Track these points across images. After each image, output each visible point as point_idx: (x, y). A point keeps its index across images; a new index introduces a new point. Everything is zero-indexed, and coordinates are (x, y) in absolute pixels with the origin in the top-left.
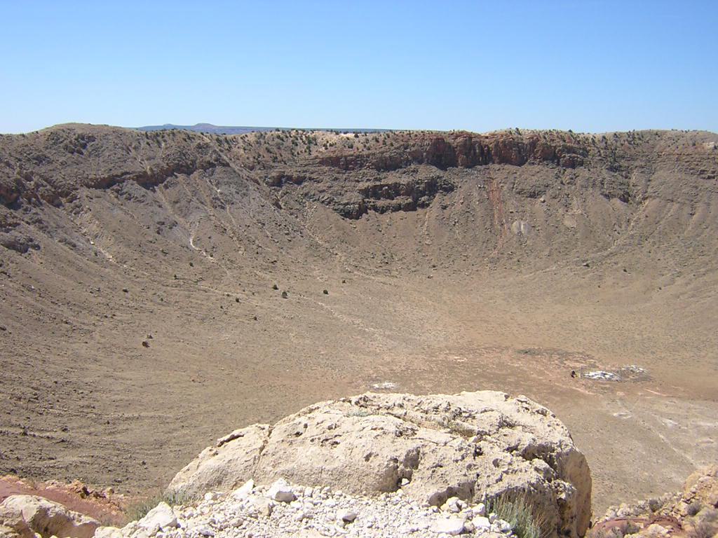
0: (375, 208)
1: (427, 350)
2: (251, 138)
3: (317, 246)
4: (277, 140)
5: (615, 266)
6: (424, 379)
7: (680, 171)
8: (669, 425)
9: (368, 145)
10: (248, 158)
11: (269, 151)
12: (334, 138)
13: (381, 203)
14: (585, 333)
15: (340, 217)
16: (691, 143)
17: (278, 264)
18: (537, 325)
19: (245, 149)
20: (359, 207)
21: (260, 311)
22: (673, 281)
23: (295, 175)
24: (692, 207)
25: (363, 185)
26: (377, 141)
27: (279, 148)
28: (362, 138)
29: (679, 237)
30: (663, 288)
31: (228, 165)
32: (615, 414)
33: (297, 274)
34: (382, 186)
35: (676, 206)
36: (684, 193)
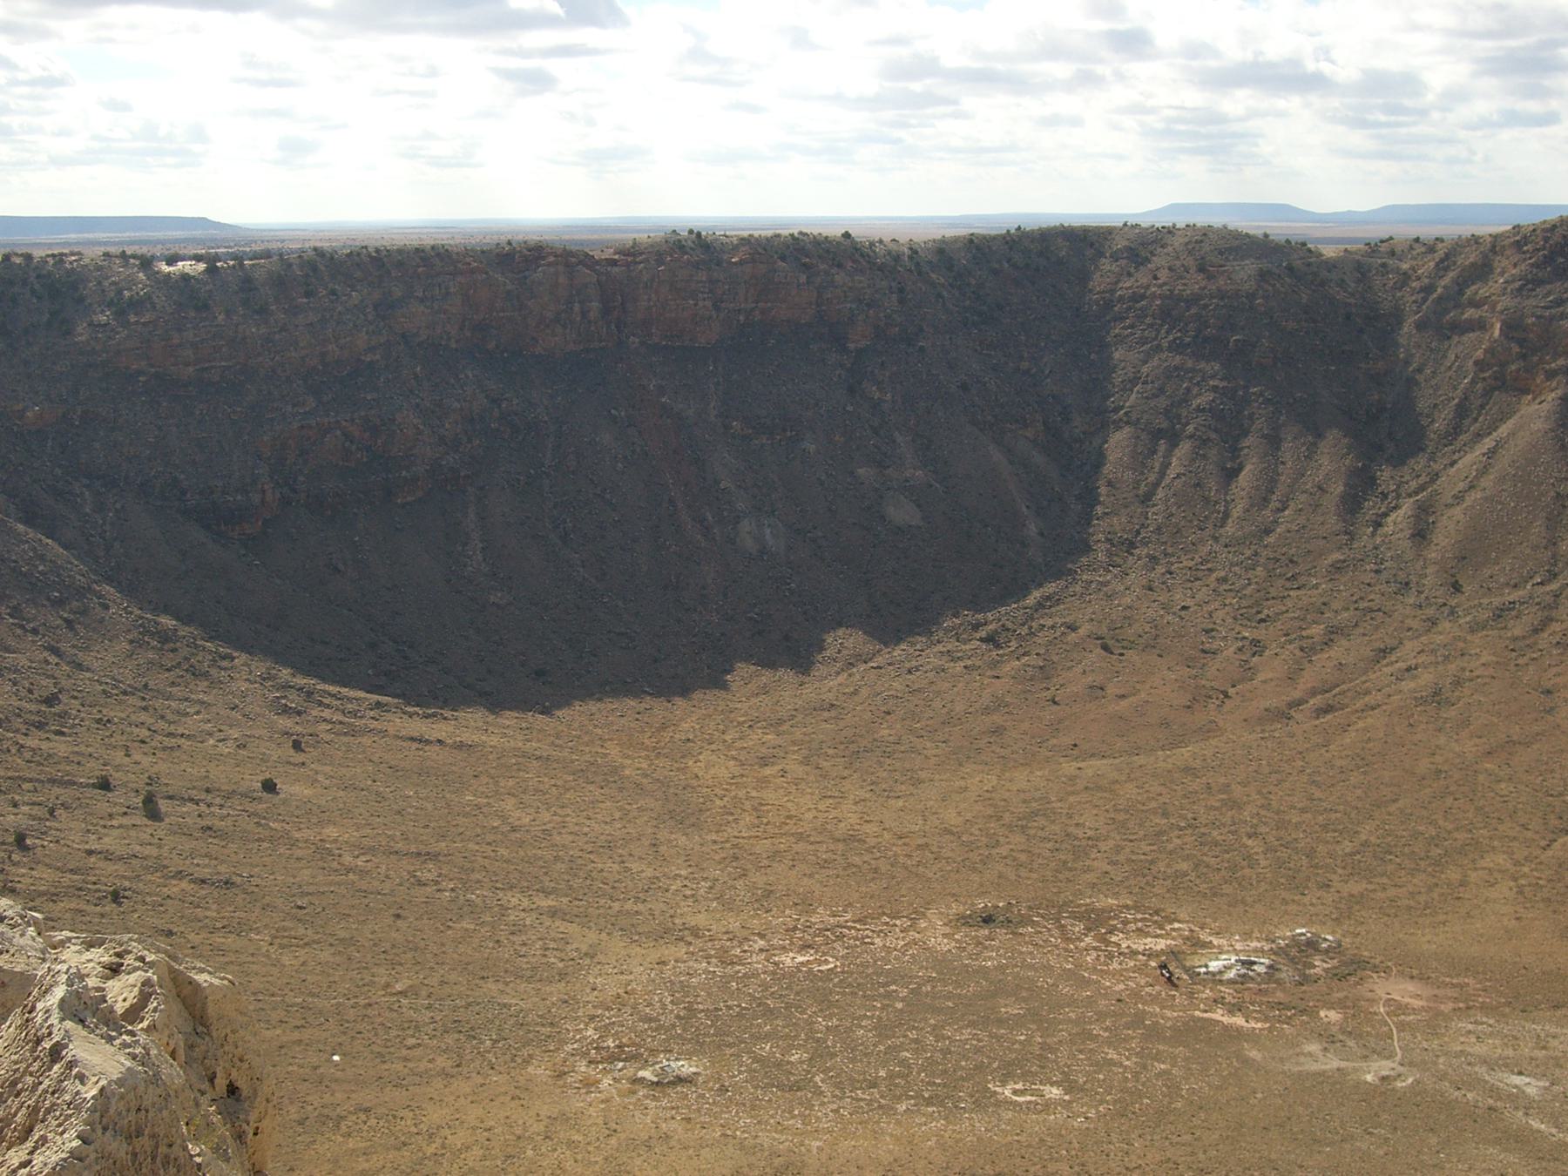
1: (699, 943)
5: (1072, 637)
6: (767, 1037)
7: (1177, 347)
8: (1529, 1090)
14: (1103, 846)
16: (1190, 262)
17: (69, 704)
18: (948, 832)
20: (263, 501)
21: (111, 867)
22: (1248, 672)
24: (1235, 451)
29: (1216, 539)
30: (1231, 691)
32: (1369, 1078)
35: (1185, 447)
36: (1198, 409)
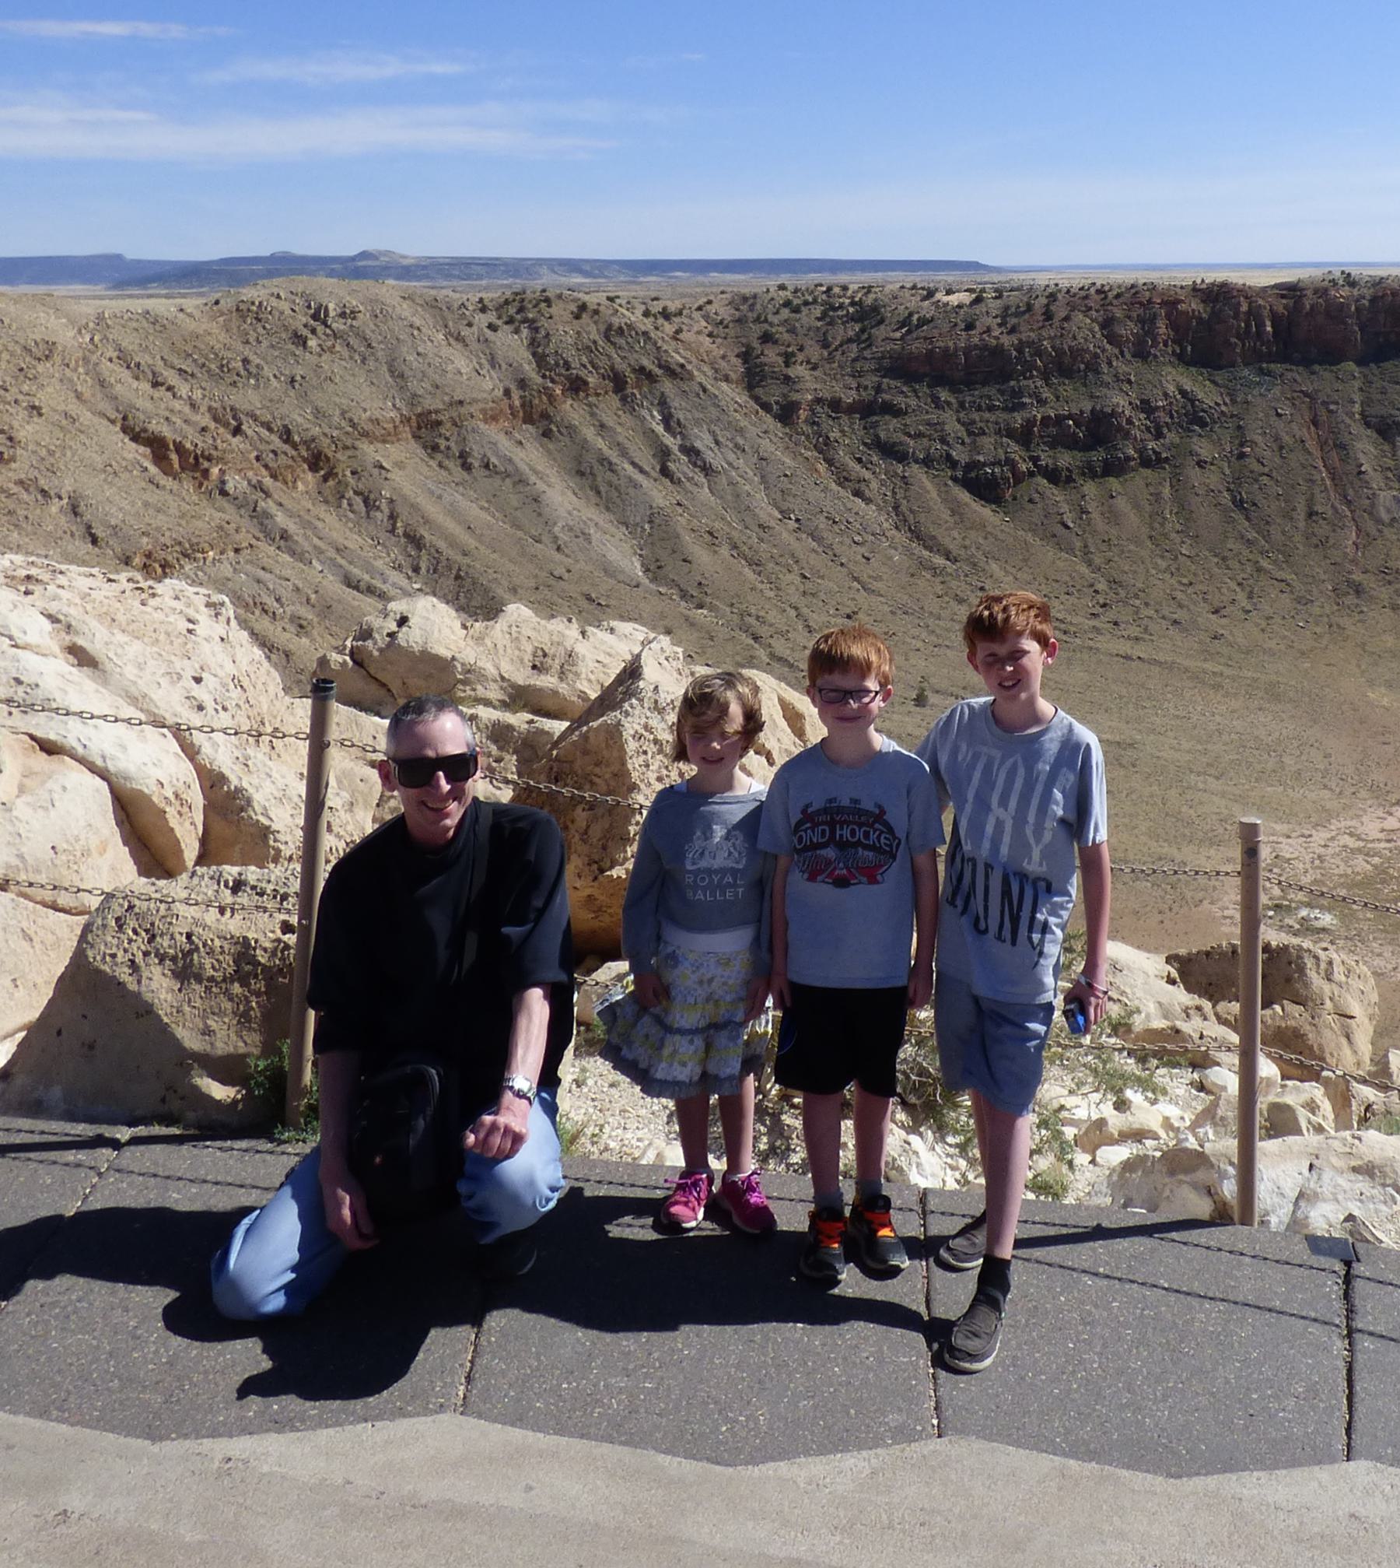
0: (1053, 476)
2: (725, 313)
3: (935, 570)
4: (785, 313)
9: (1013, 321)
10: (723, 357)
11: (767, 338)
12: (927, 309)
13: (1066, 459)
15: (965, 496)
19: (710, 335)
23: (849, 397)
25: (1018, 419)
26: (1029, 308)
27: (792, 331)
28: (995, 306)
31: (691, 377)
33: (919, 644)
34: (1060, 420)
